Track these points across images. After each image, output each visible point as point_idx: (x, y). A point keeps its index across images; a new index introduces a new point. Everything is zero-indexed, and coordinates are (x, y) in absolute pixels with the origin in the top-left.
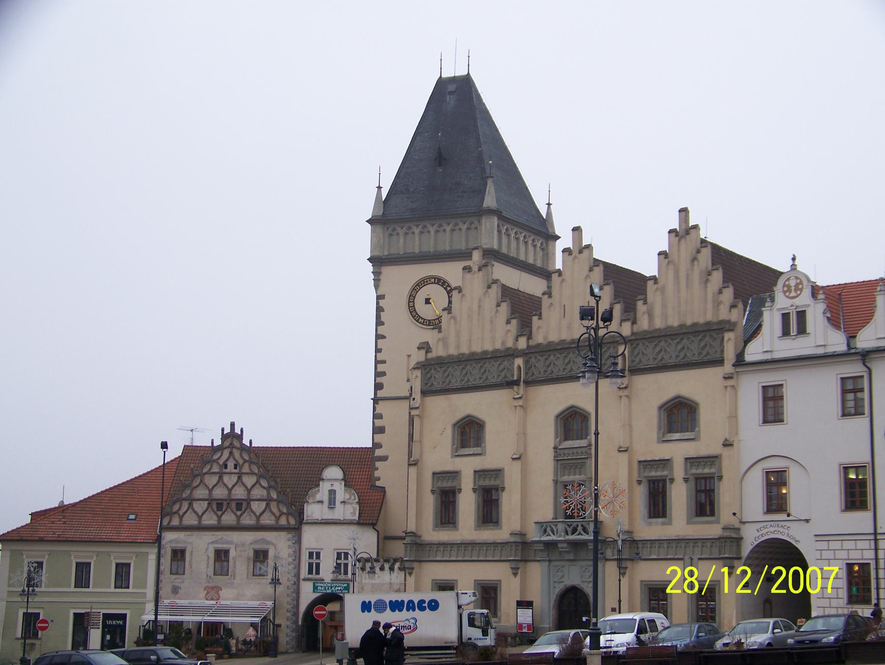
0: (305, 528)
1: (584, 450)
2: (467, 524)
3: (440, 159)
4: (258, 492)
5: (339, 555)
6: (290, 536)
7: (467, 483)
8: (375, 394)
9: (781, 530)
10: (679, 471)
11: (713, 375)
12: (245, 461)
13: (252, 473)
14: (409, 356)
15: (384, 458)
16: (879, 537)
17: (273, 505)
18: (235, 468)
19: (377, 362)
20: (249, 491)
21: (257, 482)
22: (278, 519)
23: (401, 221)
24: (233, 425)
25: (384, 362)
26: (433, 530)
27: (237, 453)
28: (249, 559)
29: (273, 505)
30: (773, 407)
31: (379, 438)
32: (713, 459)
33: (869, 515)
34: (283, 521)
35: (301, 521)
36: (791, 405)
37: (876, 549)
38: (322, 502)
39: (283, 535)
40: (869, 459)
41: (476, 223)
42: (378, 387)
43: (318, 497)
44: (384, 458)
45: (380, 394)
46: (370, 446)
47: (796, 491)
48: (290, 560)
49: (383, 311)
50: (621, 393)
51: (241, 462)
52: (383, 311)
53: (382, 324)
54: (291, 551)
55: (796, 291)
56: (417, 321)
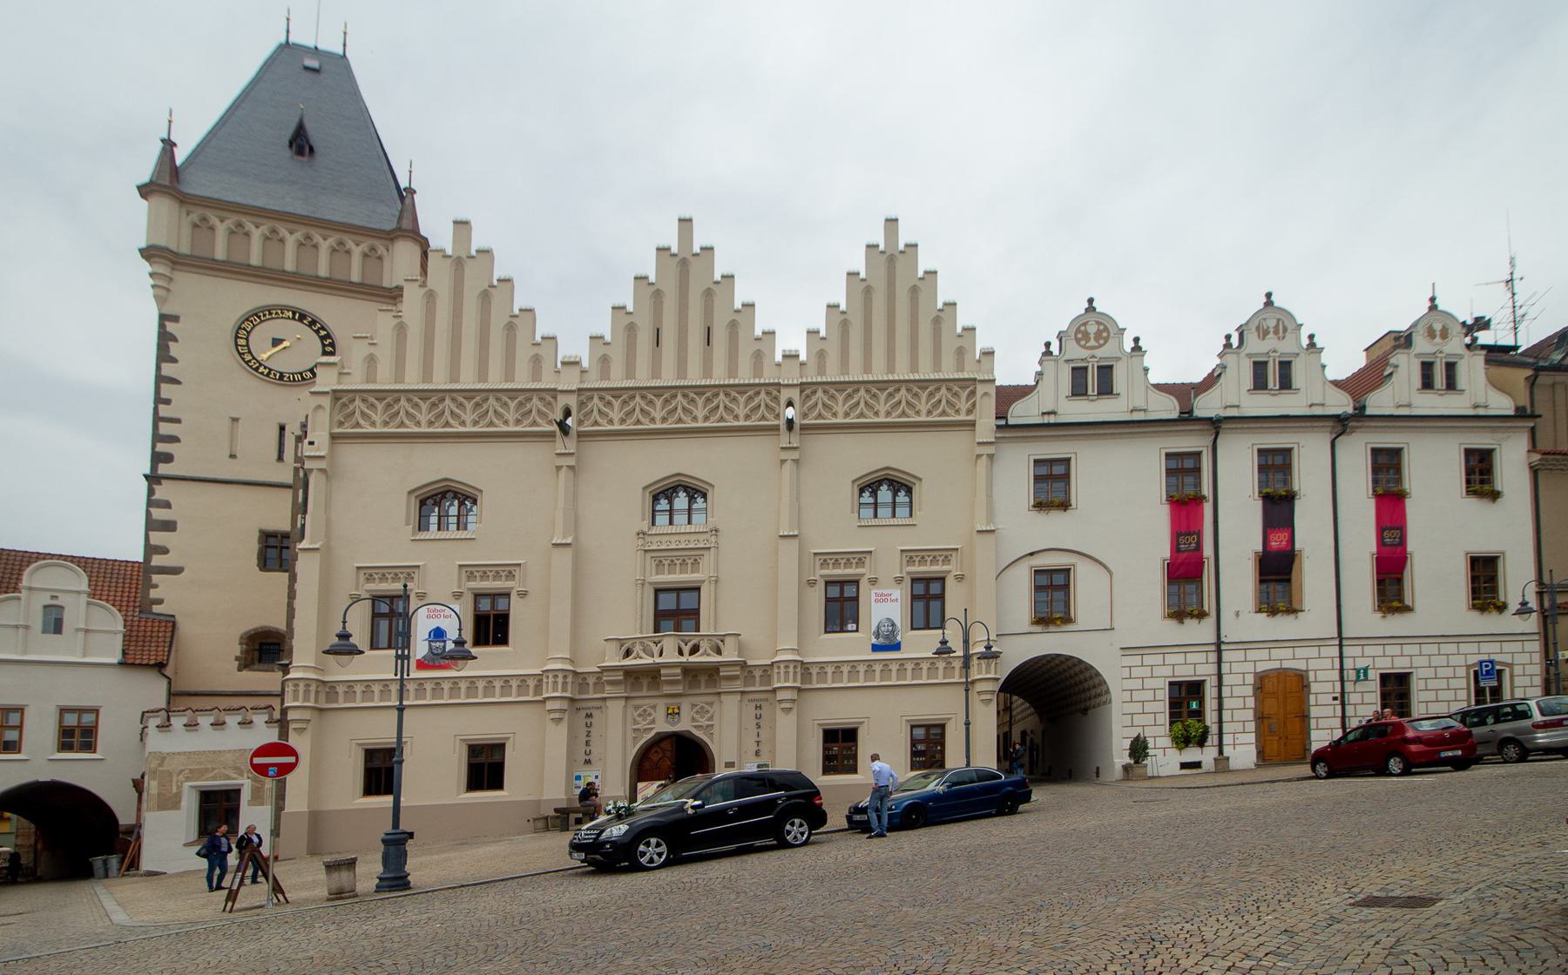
14: (235, 420)
30: (1053, 487)
33: (1210, 622)
36: (1082, 485)
37: (1219, 662)
46: (138, 556)
47: (1087, 591)
55: (1096, 339)
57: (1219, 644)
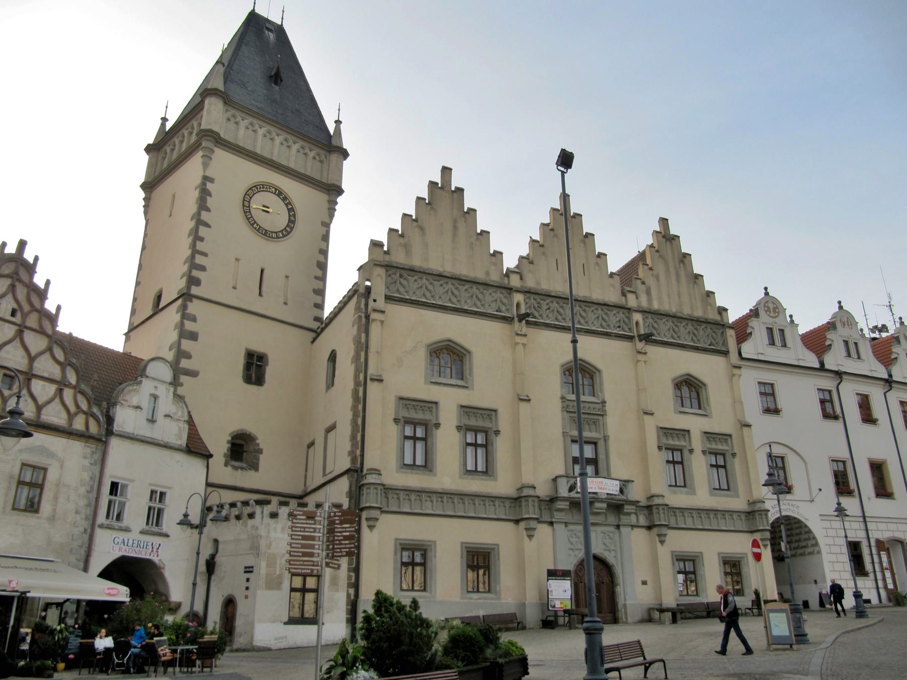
0: (115, 444)
1: (597, 406)
2: (449, 470)
3: (276, 78)
4: (46, 366)
5: (153, 492)
6: (88, 450)
7: (449, 417)
8: (188, 288)
9: (792, 508)
10: (697, 443)
11: (718, 361)
12: (34, 309)
13: (41, 331)
15: (194, 374)
16: (867, 519)
17: (68, 394)
18: (13, 313)
19: (195, 252)
20: (32, 359)
21: (50, 349)
22: (71, 417)
23: (247, 111)
24: (22, 244)
25: (205, 255)
26: (397, 472)
27: (21, 292)
28: (11, 477)
29: (68, 394)
31: (186, 345)
32: (725, 437)
34: (79, 424)
35: (110, 432)
38: (138, 407)
39: (77, 448)
40: (848, 456)
41: (323, 157)
42: (193, 281)
43: (135, 401)
44: (194, 374)
45: (195, 290)
47: (795, 474)
48: (83, 490)
49: (210, 195)
50: (640, 357)
51: (26, 308)
52: (210, 195)
53: (208, 210)
54: (86, 476)
55: (774, 312)
56: (252, 225)
57: (864, 517)
